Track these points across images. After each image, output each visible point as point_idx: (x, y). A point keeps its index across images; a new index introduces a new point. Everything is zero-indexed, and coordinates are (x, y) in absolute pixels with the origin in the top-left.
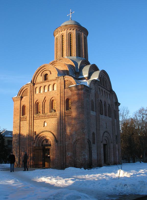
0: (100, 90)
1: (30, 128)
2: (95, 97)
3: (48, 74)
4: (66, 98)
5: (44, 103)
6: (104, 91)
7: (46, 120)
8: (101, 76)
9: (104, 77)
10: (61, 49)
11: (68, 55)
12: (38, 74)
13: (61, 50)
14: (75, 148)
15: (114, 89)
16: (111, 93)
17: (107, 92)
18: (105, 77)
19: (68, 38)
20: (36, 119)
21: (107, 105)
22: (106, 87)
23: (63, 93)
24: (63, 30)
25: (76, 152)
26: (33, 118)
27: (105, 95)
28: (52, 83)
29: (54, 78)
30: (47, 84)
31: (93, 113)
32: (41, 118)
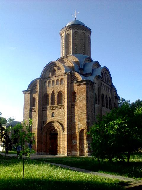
0: (102, 85)
2: (98, 91)
3: (56, 71)
6: (106, 86)
7: (54, 111)
8: (103, 72)
15: (114, 84)
16: (111, 88)
17: (108, 87)
20: (45, 110)
21: (108, 99)
22: (108, 82)
27: (106, 90)
28: (60, 78)
29: (62, 74)
31: (97, 106)
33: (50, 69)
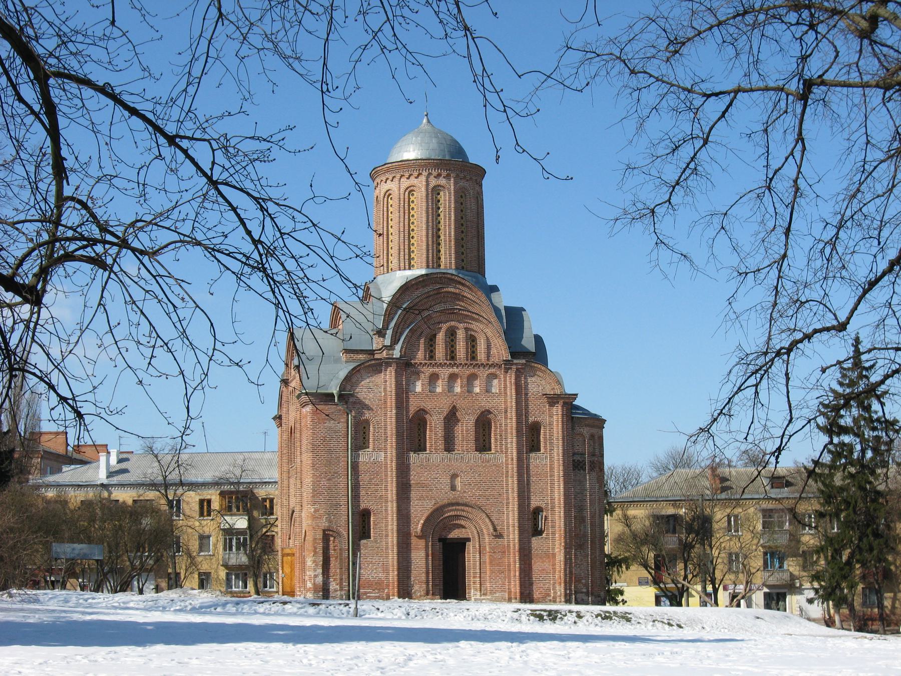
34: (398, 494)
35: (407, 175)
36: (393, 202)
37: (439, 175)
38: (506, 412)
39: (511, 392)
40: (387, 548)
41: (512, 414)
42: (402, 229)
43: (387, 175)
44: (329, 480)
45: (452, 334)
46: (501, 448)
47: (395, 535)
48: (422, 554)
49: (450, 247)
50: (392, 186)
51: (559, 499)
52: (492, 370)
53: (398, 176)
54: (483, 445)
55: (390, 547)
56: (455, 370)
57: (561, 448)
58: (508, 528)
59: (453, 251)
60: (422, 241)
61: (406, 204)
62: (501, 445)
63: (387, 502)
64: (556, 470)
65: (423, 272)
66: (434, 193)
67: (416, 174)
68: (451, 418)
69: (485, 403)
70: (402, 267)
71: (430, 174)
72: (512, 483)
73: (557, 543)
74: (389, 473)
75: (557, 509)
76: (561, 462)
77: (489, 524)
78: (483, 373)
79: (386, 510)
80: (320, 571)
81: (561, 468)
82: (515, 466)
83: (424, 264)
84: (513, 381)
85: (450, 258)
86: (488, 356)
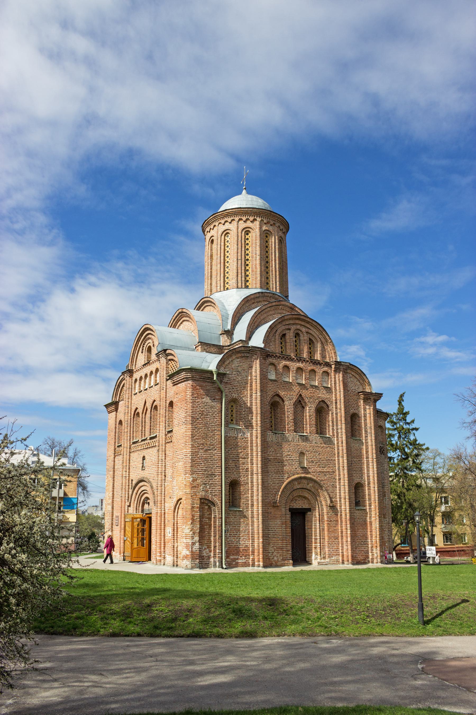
1: (124, 473)
4: (168, 402)
5: (144, 414)
7: (145, 453)
9: (301, 331)
10: (209, 275)
11: (219, 288)
12: (138, 349)
13: (209, 278)
14: (176, 519)
18: (304, 330)
19: (219, 246)
23: (165, 390)
24: (212, 227)
25: (177, 528)
26: (130, 448)
30: (147, 370)
32: (139, 449)
33: (143, 347)
34: (262, 468)
35: (244, 219)
36: (232, 239)
37: (268, 223)
38: (336, 403)
39: (340, 387)
40: (253, 517)
41: (341, 406)
42: (239, 258)
43: (226, 219)
44: (206, 450)
45: (297, 335)
46: (333, 433)
47: (260, 504)
48: (278, 522)
49: (276, 276)
50: (233, 227)
51: (374, 477)
52: (326, 369)
53: (237, 219)
54: (320, 428)
55: (255, 516)
56: (300, 365)
57: (373, 436)
58: (340, 501)
59: (278, 280)
60: (256, 268)
61: (243, 240)
62: (333, 430)
63: (252, 474)
64: (370, 453)
65: (259, 290)
66: (265, 236)
67: (251, 218)
68: (300, 403)
69: (323, 395)
70: (240, 286)
71: (262, 220)
72: (343, 461)
73: (373, 513)
74: (254, 448)
75: (372, 485)
76: (374, 447)
77: (327, 496)
78: (320, 370)
79: (252, 482)
80: (197, 538)
81: (374, 451)
82: (345, 448)
83: (258, 285)
84: (341, 379)
85: (276, 284)
86: (323, 356)
